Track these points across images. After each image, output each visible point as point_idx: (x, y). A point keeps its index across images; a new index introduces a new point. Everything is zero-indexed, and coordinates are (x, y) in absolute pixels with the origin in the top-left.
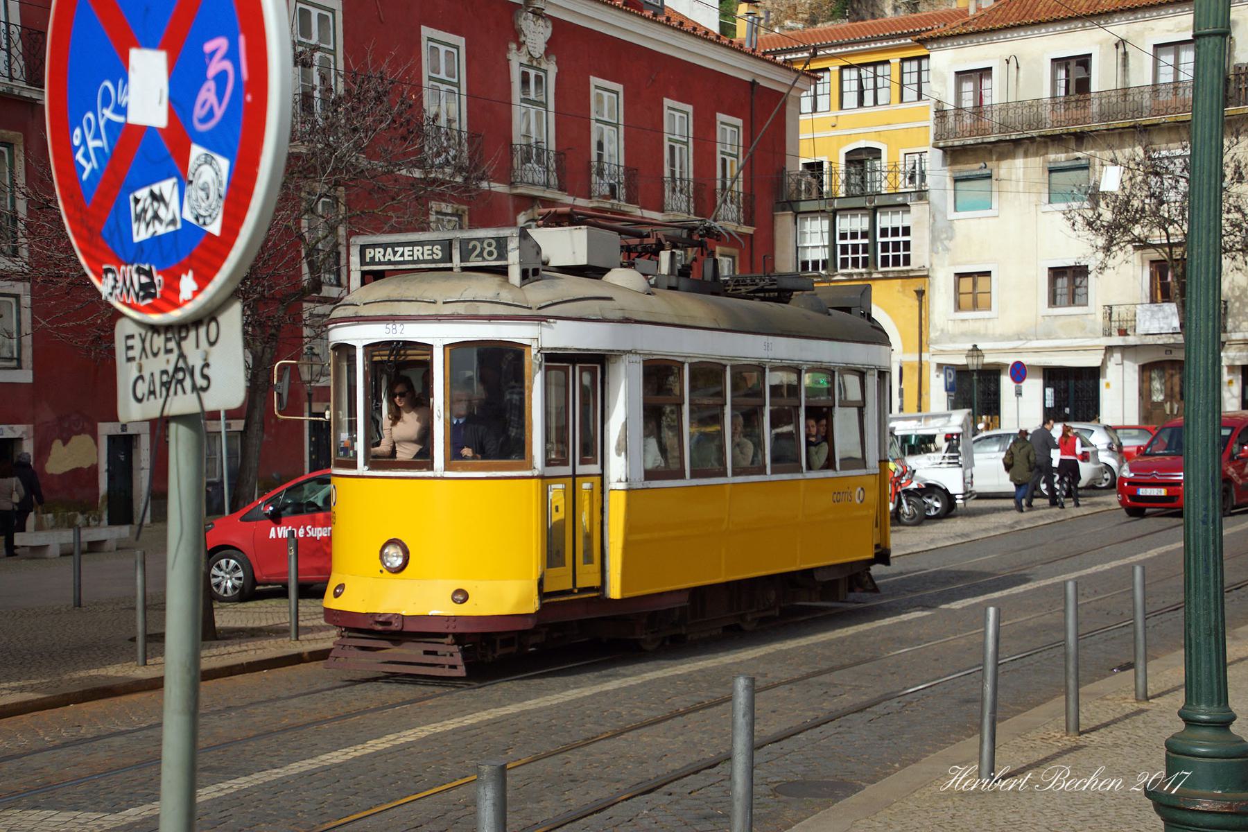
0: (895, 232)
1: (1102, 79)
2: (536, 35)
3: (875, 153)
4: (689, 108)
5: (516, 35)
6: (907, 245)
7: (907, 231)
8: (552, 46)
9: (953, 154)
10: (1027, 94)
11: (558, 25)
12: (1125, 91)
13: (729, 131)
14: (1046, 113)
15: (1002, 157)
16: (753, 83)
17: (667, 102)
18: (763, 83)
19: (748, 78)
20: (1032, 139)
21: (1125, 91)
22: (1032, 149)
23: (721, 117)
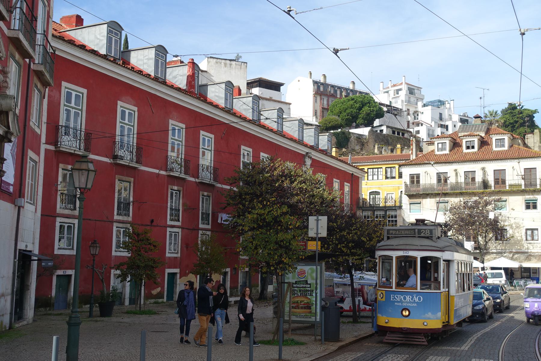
0: (392, 217)
1: (452, 180)
2: (308, 162)
3: (378, 193)
4: (339, 181)
5: (304, 163)
6: (396, 221)
7: (396, 217)
8: (312, 166)
9: (410, 196)
10: (432, 182)
11: (314, 161)
12: (457, 183)
13: (347, 188)
14: (435, 187)
15: (423, 198)
16: (352, 174)
17: (334, 180)
18: (355, 174)
19: (351, 173)
20: (432, 194)
21: (457, 183)
22: (432, 196)
23: (346, 183)
